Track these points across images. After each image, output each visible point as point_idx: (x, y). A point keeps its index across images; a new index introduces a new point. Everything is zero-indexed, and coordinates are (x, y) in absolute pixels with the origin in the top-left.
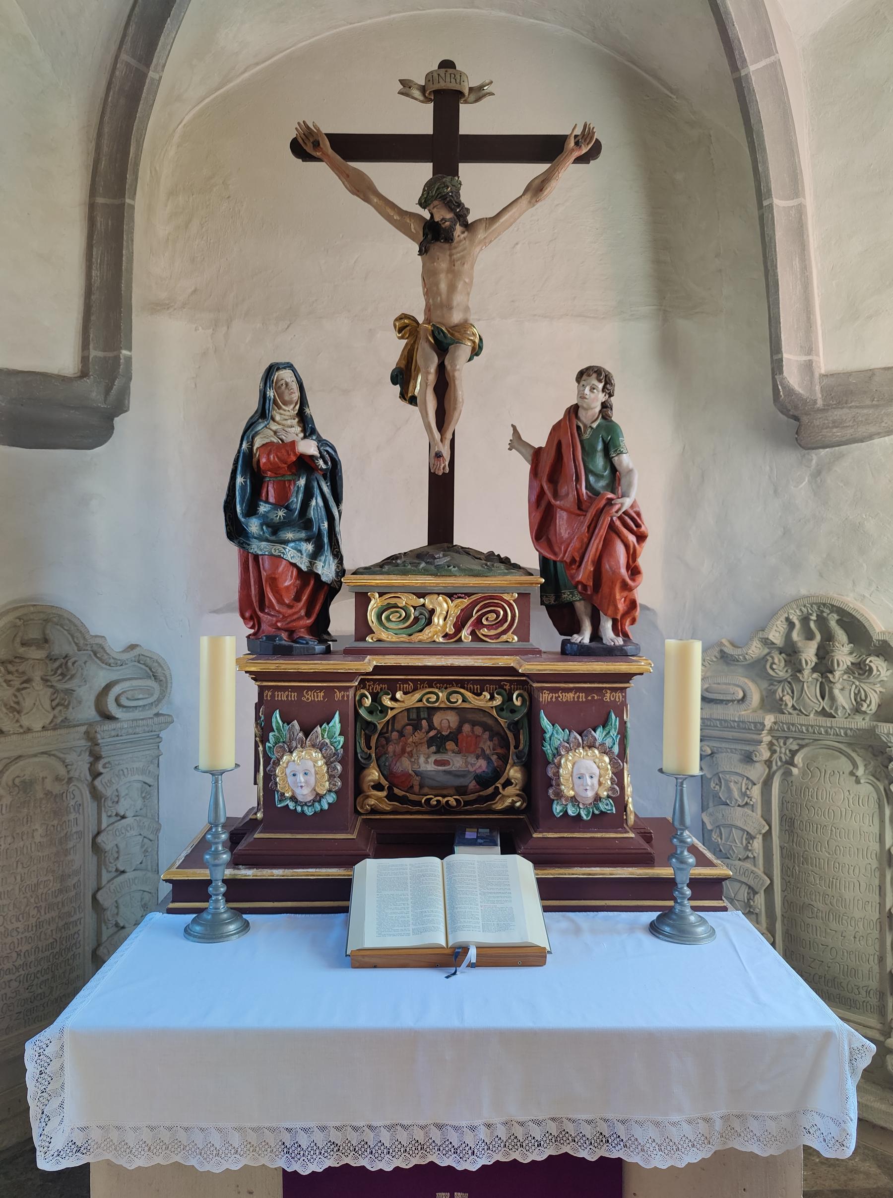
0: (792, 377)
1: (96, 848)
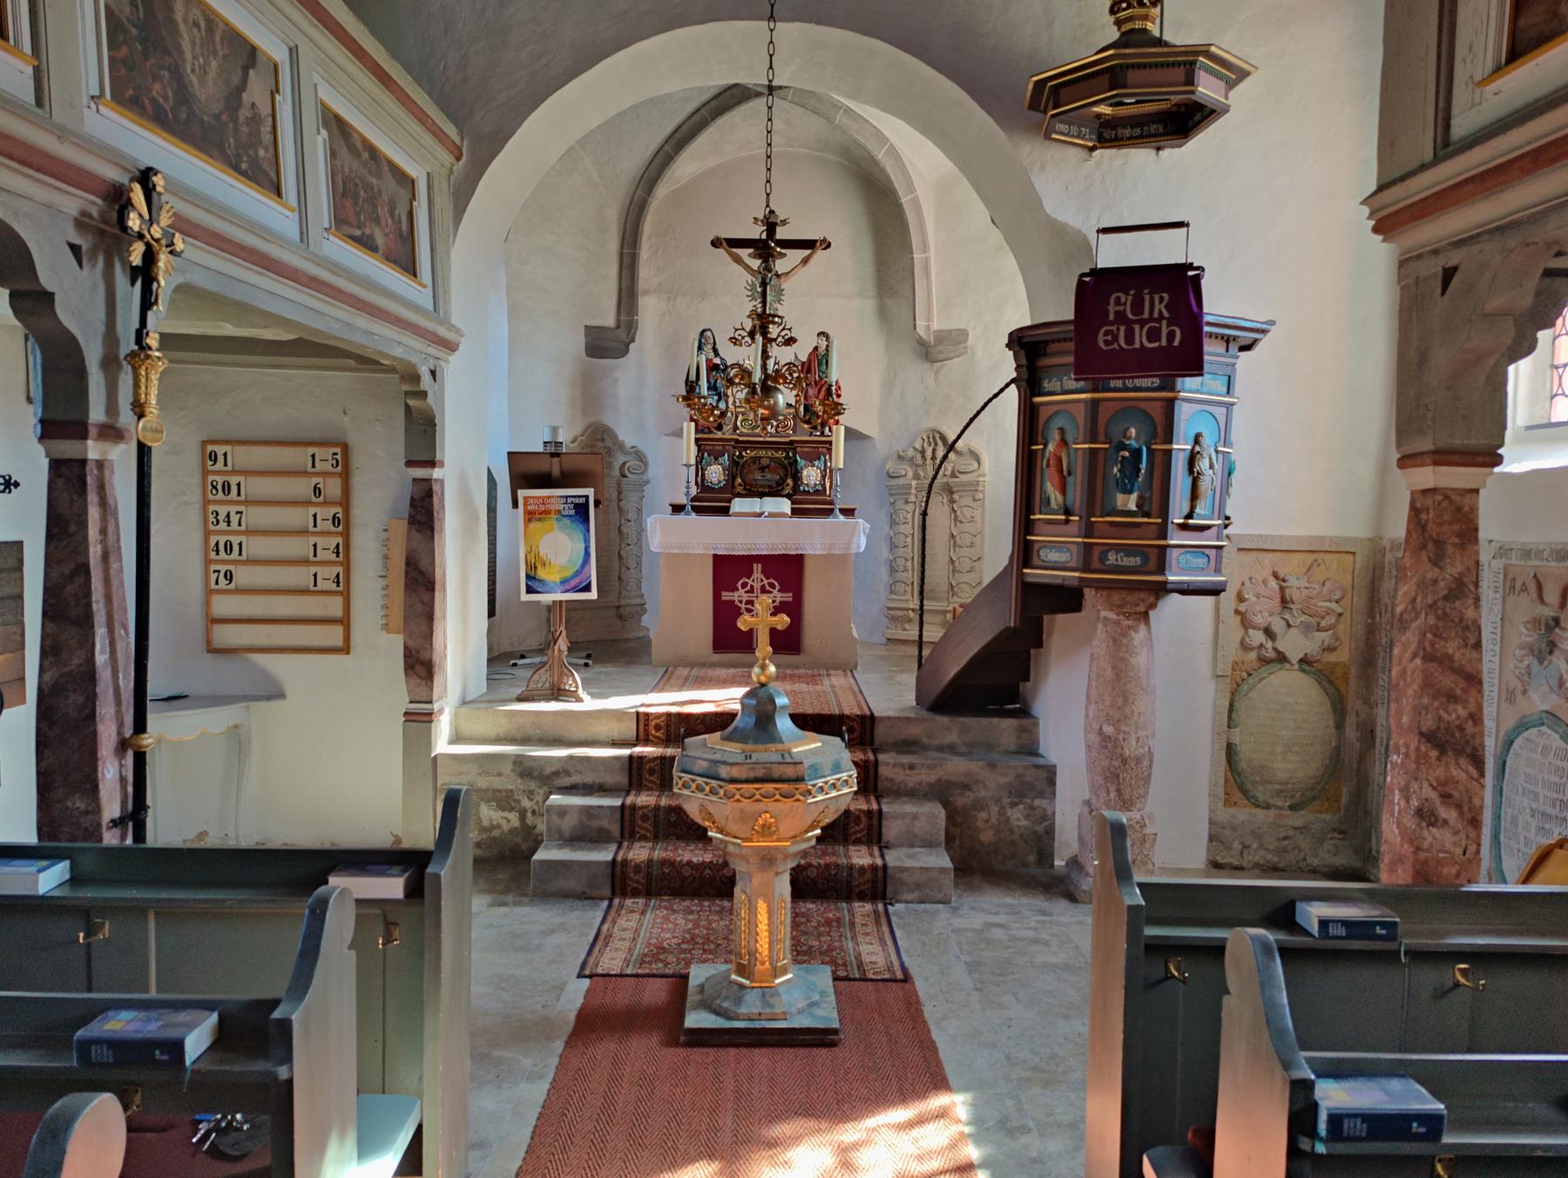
0: (921, 331)
1: (620, 532)
